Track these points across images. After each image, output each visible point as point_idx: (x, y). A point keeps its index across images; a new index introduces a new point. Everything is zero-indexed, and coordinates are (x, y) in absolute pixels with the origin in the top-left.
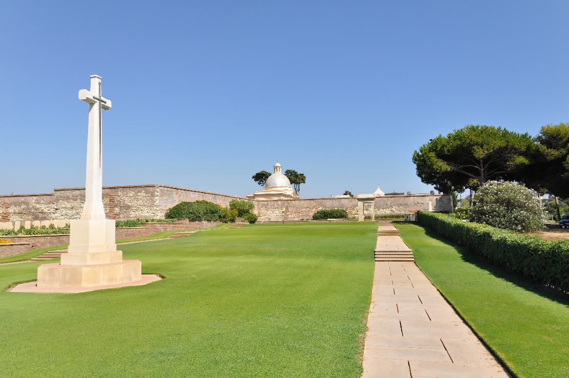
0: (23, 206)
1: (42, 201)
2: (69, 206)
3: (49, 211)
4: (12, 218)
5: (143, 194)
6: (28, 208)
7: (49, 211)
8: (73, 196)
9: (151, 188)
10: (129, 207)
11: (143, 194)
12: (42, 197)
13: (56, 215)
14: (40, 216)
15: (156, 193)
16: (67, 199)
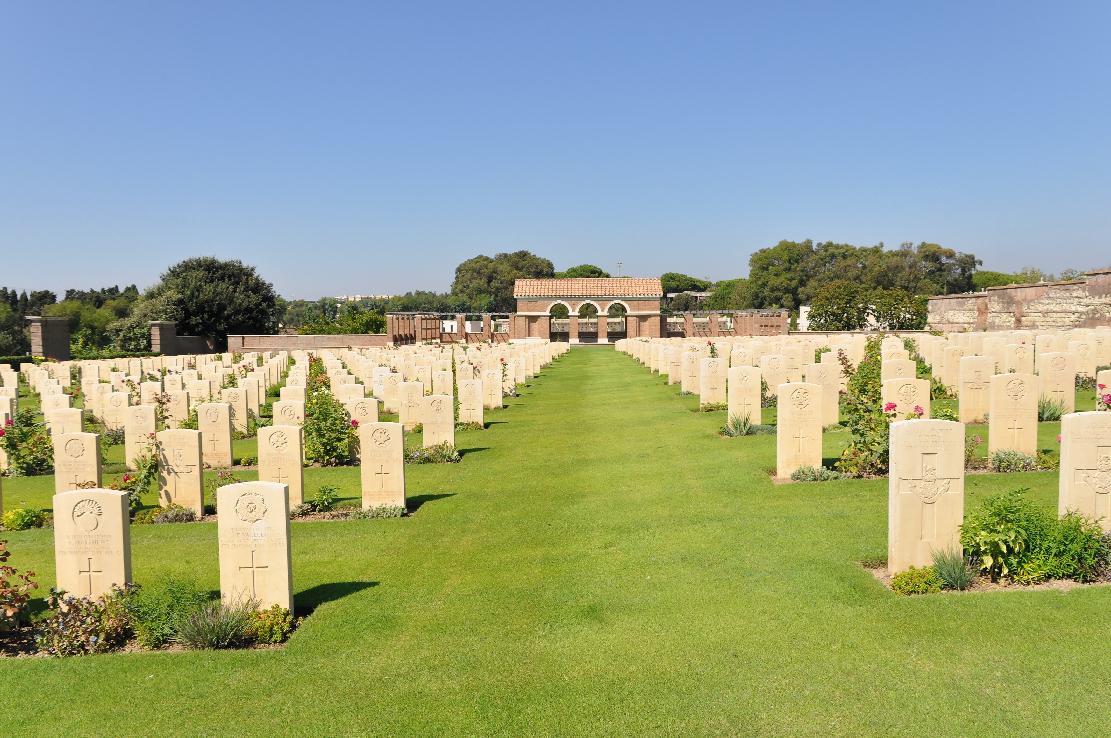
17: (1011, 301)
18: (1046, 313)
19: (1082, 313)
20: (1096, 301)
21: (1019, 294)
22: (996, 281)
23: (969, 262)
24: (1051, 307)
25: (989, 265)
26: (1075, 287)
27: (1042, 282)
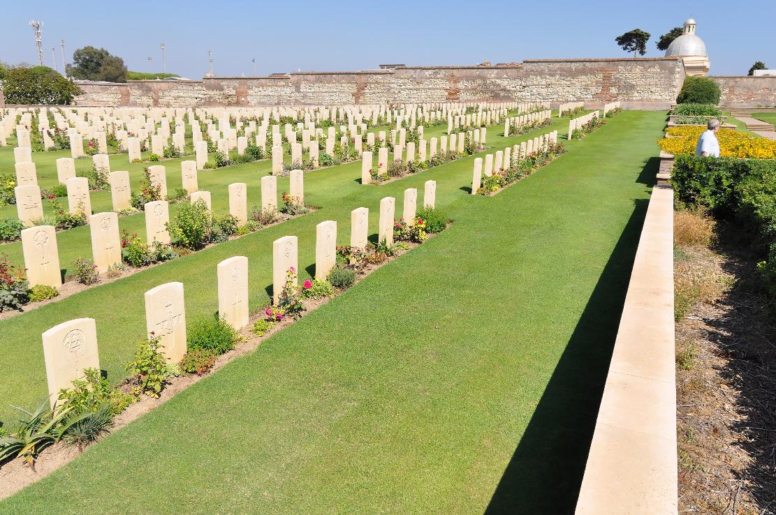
0: (479, 82)
1: (505, 76)
2: (544, 83)
3: (514, 89)
4: (463, 96)
5: (657, 69)
6: (485, 84)
7: (514, 89)
8: (549, 70)
9: (671, 63)
10: (632, 87)
11: (657, 69)
12: (505, 71)
13: (523, 93)
14: (502, 94)
15: (677, 70)
16: (541, 73)
17: (149, 90)
18: (177, 98)
19: (202, 99)
20: (211, 93)
21: (155, 86)
22: (138, 79)
23: (119, 62)
24: (181, 94)
25: (132, 66)
26: (196, 84)
27: (158, 80)
